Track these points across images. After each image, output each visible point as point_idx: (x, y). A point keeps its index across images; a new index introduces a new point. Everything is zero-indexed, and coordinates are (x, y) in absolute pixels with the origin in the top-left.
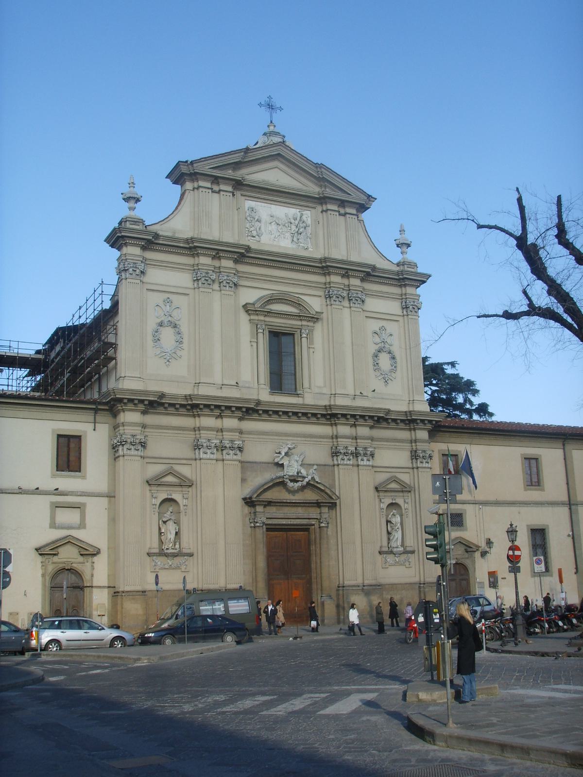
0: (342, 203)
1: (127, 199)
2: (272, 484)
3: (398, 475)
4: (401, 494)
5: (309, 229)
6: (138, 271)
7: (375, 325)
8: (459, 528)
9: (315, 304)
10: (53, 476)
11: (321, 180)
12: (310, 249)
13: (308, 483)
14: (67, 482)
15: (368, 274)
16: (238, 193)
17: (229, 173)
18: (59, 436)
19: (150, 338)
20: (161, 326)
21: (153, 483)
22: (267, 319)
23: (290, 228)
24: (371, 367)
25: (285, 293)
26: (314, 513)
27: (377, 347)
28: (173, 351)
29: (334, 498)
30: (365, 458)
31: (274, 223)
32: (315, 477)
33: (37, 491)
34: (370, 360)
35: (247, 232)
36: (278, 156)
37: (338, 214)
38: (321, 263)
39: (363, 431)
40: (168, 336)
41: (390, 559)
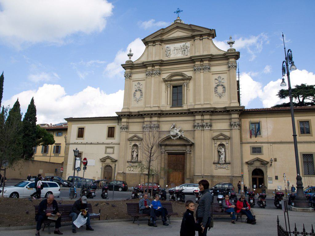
0: (201, 36)
1: (128, 55)
2: (166, 138)
3: (223, 133)
4: (225, 140)
5: (189, 49)
6: (128, 76)
7: (216, 76)
8: (259, 154)
9: (189, 74)
10: (107, 139)
11: (193, 30)
13: (180, 137)
14: (110, 140)
15: (210, 58)
16: (163, 44)
17: (159, 38)
18: (109, 128)
19: (133, 95)
21: (131, 140)
22: (171, 83)
24: (214, 92)
25: (179, 72)
26: (184, 148)
27: (217, 84)
30: (207, 127)
33: (103, 144)
34: (213, 90)
36: (177, 27)
37: (199, 40)
38: (191, 59)
39: (207, 117)
40: (138, 93)
41: (218, 165)
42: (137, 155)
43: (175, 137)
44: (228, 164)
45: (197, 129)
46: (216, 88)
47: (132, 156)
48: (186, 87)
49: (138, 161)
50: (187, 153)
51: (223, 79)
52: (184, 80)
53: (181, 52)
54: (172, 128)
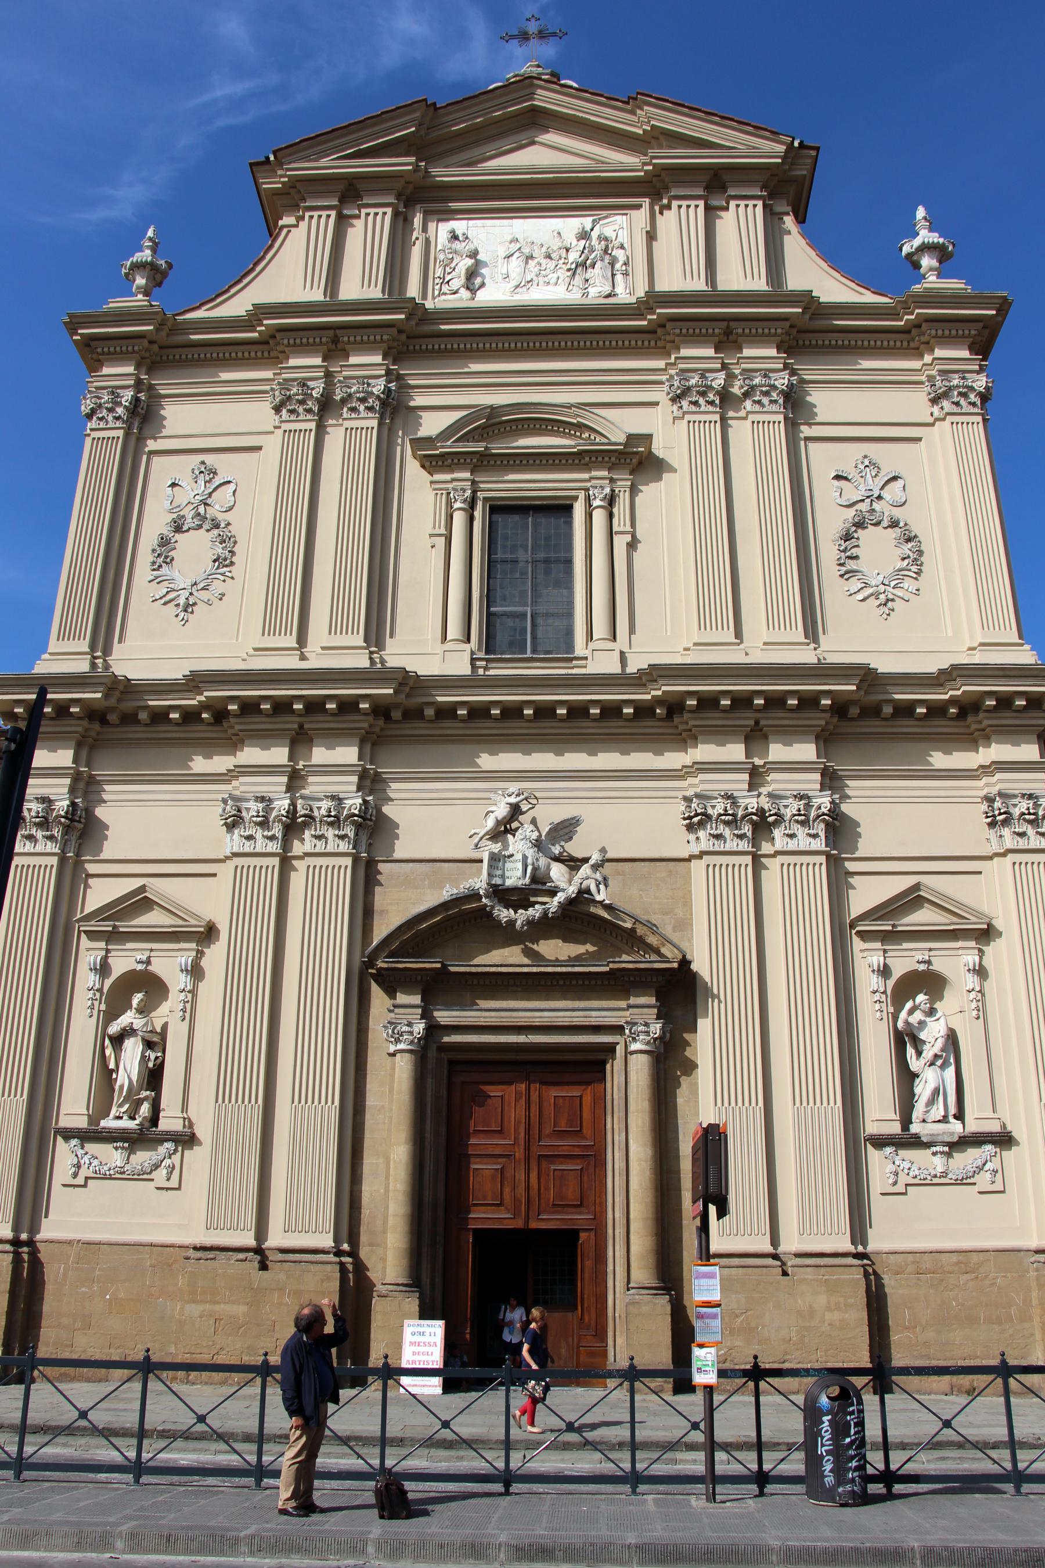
12: (620, 296)
20: (178, 529)
23: (563, 261)
27: (852, 512)
28: (202, 585)
29: (669, 955)
30: (801, 832)
31: (517, 254)
32: (593, 888)
35: (437, 287)
42: (154, 1077)
43: (527, 905)
44: (989, 1148)
45: (719, 846)
46: (847, 537)
47: (105, 1076)
48: (599, 517)
49: (164, 1125)
50: (628, 1053)
51: (895, 478)
52: (587, 468)
53: (563, 274)
54: (490, 823)
